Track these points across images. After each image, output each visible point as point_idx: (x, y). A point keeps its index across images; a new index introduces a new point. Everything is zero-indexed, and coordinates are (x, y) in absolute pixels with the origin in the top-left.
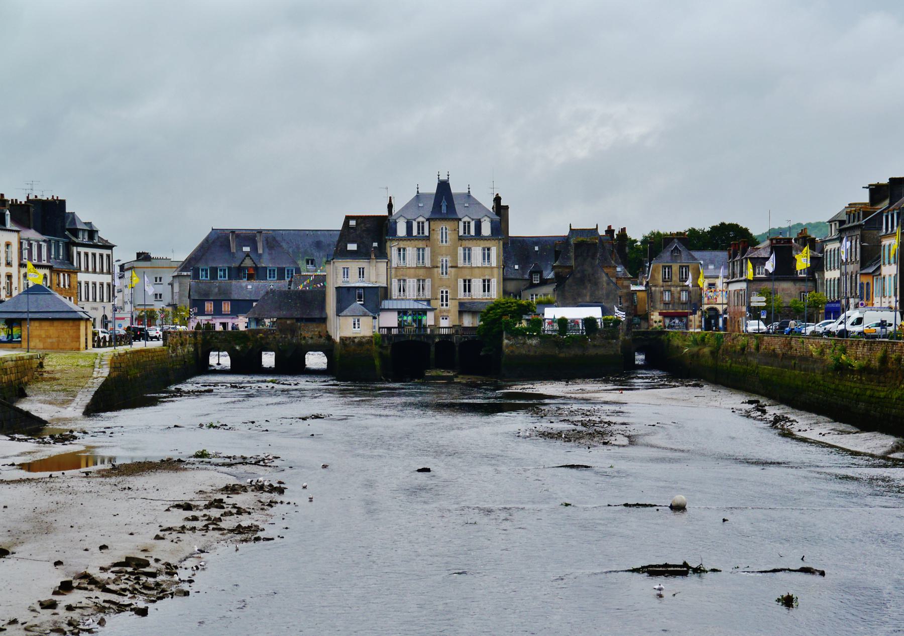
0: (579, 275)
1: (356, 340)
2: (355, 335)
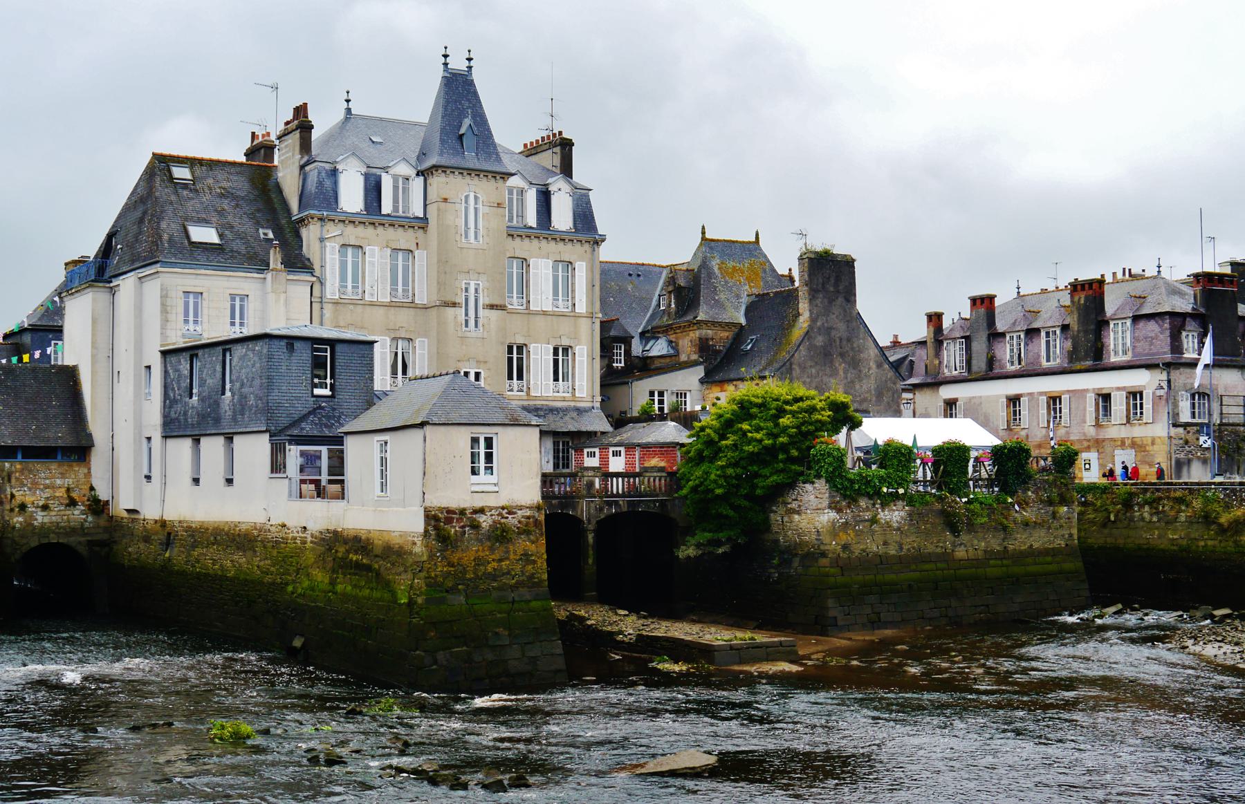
0: (819, 340)
1: (485, 521)
2: (478, 502)
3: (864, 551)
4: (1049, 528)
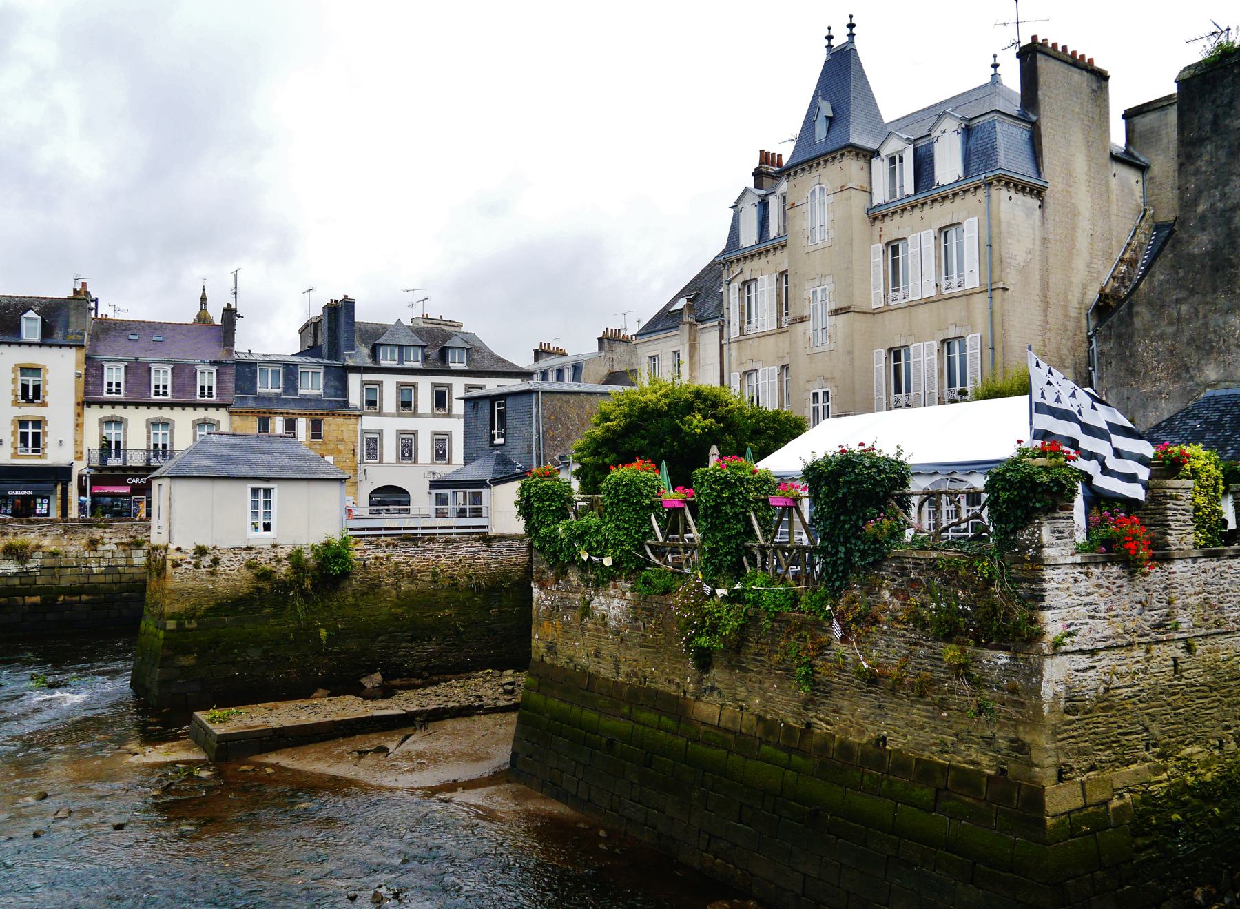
0: (1202, 243)
3: (571, 659)
4: (942, 705)
